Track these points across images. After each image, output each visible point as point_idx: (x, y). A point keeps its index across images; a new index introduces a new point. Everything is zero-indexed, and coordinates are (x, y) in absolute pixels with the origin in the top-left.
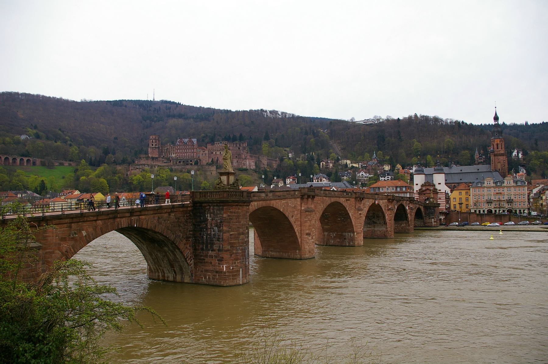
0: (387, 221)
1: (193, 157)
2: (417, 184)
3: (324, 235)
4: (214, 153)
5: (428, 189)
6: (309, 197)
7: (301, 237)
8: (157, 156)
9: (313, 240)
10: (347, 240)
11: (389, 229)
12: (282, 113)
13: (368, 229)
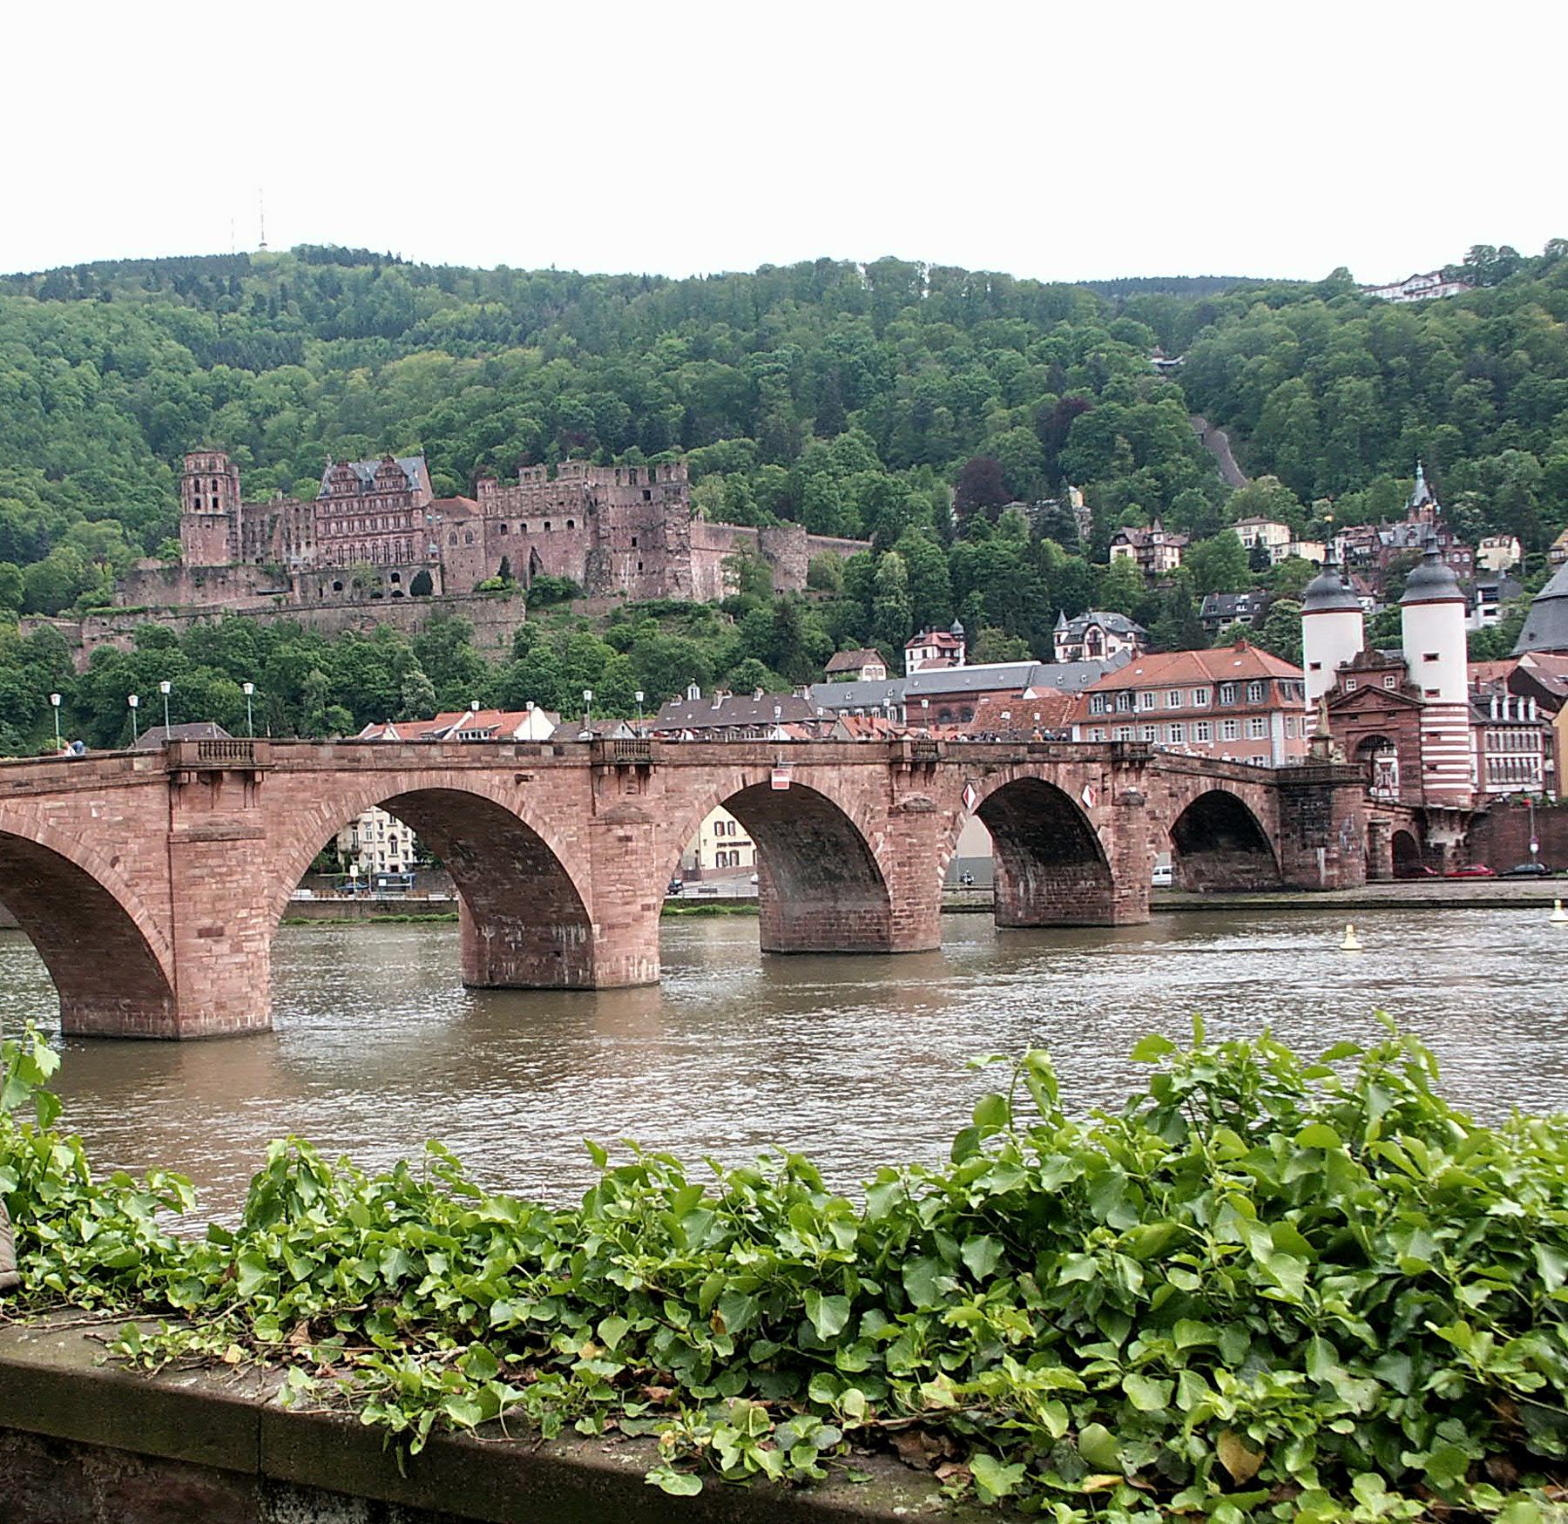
0: (884, 867)
3: (481, 940)
4: (516, 526)
5: (1369, 689)
6: (213, 778)
7: (172, 945)
8: (224, 561)
9: (240, 958)
10: (565, 959)
11: (897, 905)
13: (812, 907)
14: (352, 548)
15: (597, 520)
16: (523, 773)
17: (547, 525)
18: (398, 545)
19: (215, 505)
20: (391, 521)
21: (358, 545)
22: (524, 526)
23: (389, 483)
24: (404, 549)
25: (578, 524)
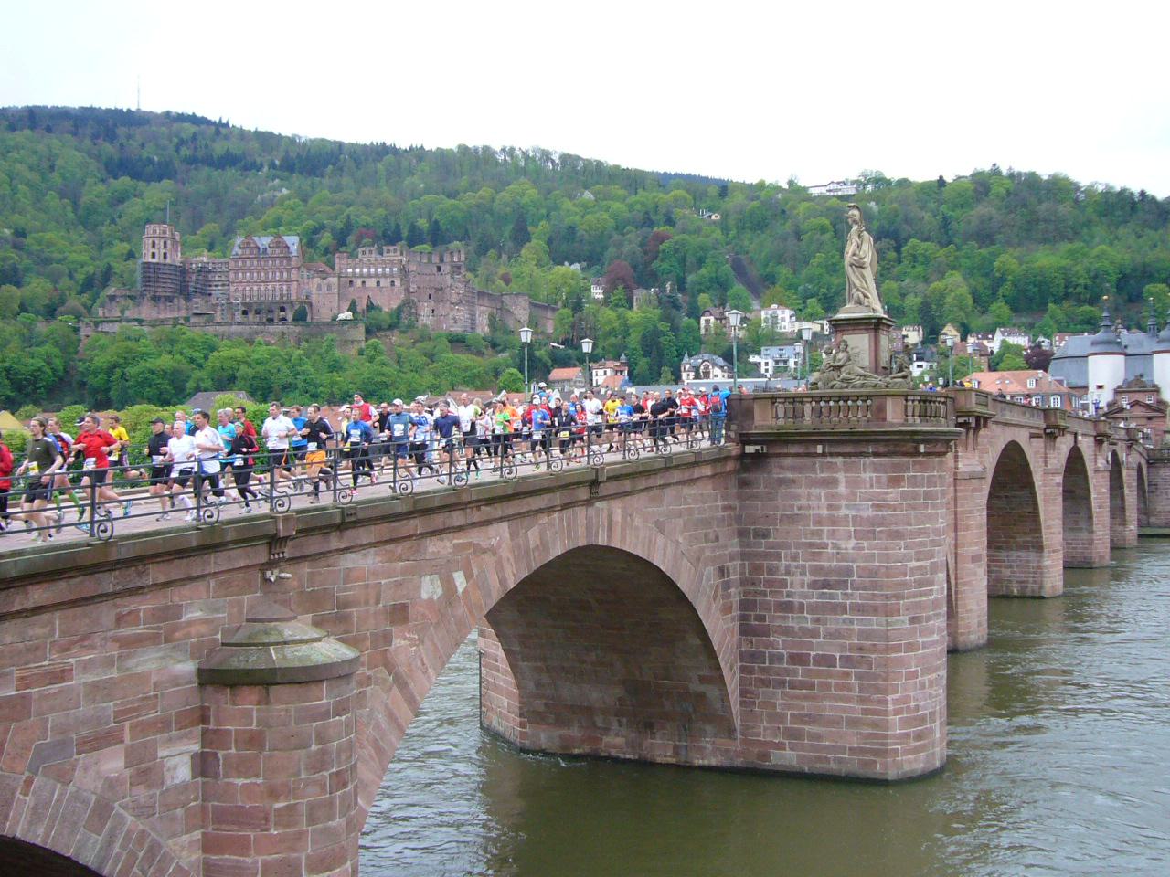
1: (289, 295)
2: (1100, 387)
4: (359, 282)
12: (566, 158)
14: (251, 290)
15: (408, 282)
16: (1032, 431)
17: (378, 283)
18: (281, 290)
19: (165, 255)
20: (278, 274)
21: (255, 288)
22: (364, 282)
23: (278, 251)
24: (285, 292)
25: (398, 283)
